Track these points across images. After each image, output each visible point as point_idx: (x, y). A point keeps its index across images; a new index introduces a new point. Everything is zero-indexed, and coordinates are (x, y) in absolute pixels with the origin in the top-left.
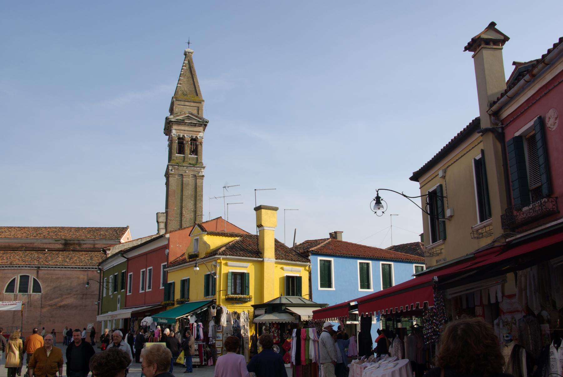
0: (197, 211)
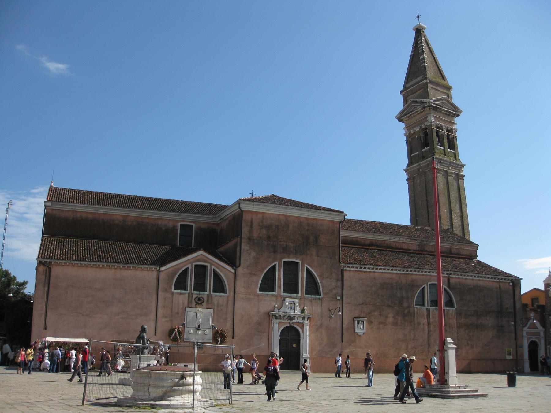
0: (463, 216)
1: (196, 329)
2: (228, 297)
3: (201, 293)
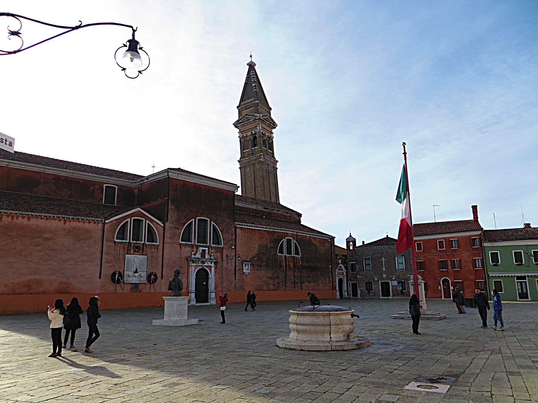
1: (134, 272)
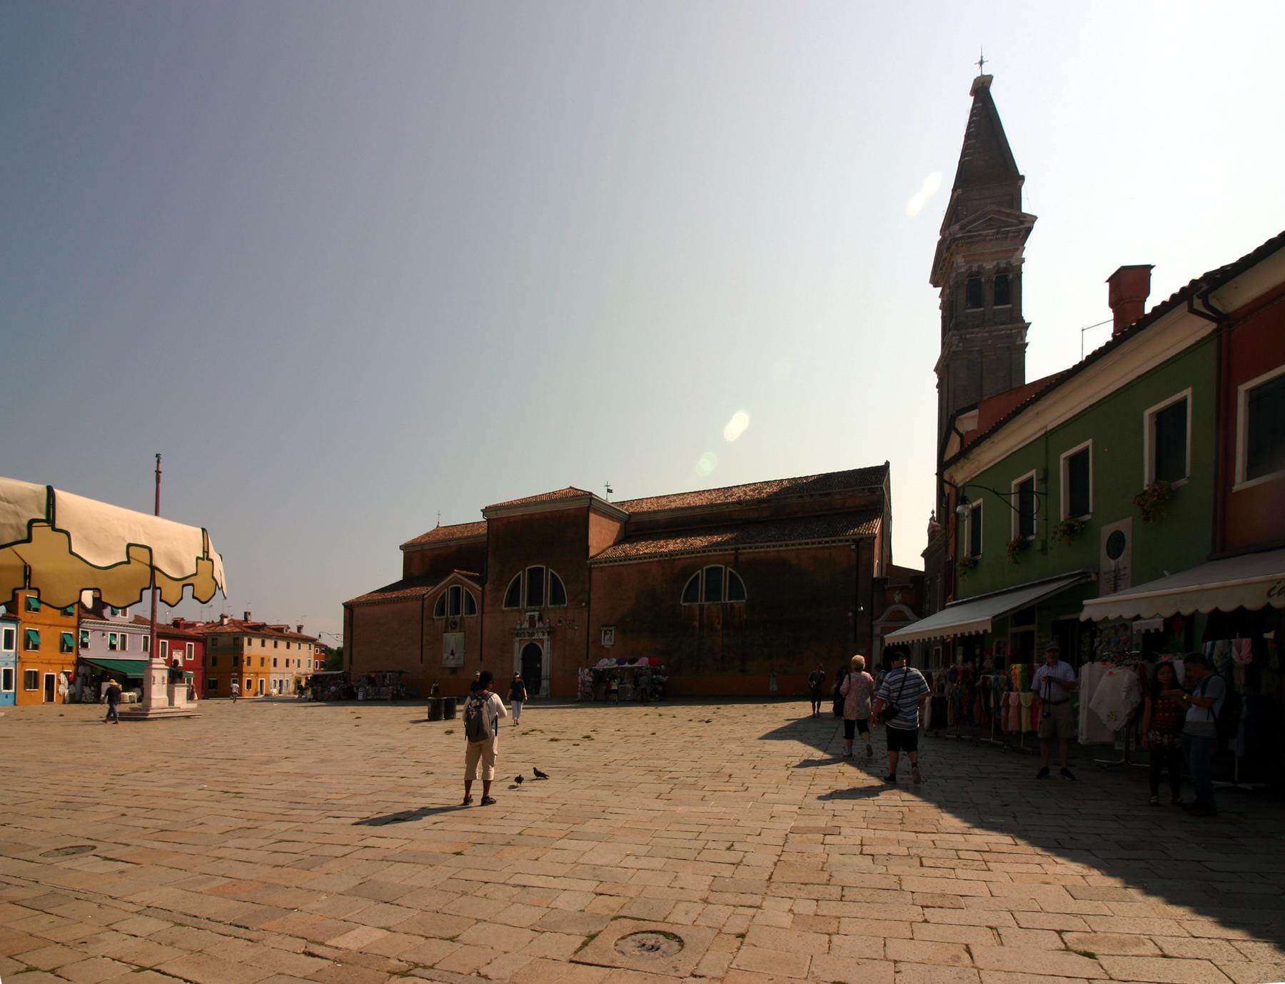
2: (477, 617)
3: (456, 616)
